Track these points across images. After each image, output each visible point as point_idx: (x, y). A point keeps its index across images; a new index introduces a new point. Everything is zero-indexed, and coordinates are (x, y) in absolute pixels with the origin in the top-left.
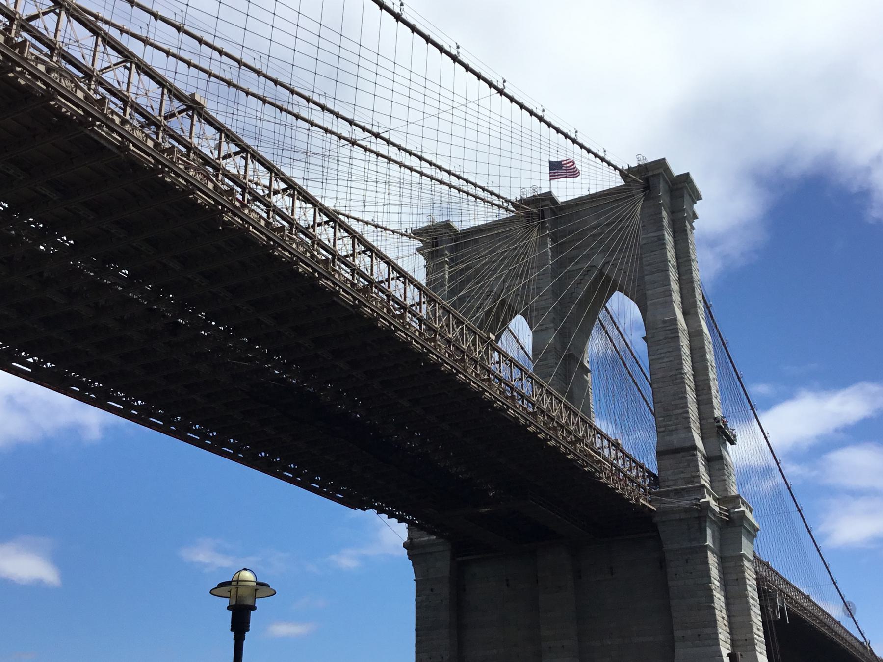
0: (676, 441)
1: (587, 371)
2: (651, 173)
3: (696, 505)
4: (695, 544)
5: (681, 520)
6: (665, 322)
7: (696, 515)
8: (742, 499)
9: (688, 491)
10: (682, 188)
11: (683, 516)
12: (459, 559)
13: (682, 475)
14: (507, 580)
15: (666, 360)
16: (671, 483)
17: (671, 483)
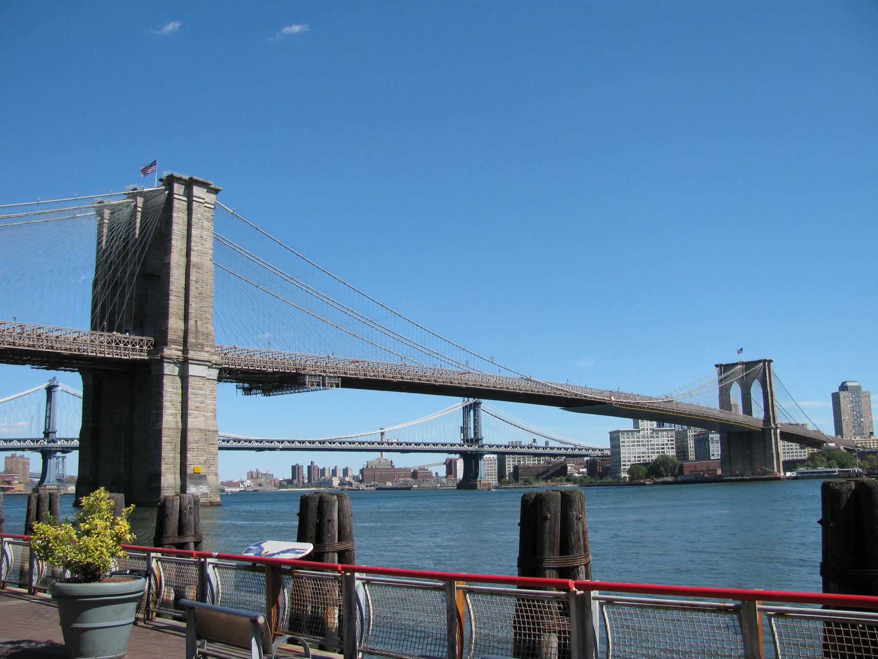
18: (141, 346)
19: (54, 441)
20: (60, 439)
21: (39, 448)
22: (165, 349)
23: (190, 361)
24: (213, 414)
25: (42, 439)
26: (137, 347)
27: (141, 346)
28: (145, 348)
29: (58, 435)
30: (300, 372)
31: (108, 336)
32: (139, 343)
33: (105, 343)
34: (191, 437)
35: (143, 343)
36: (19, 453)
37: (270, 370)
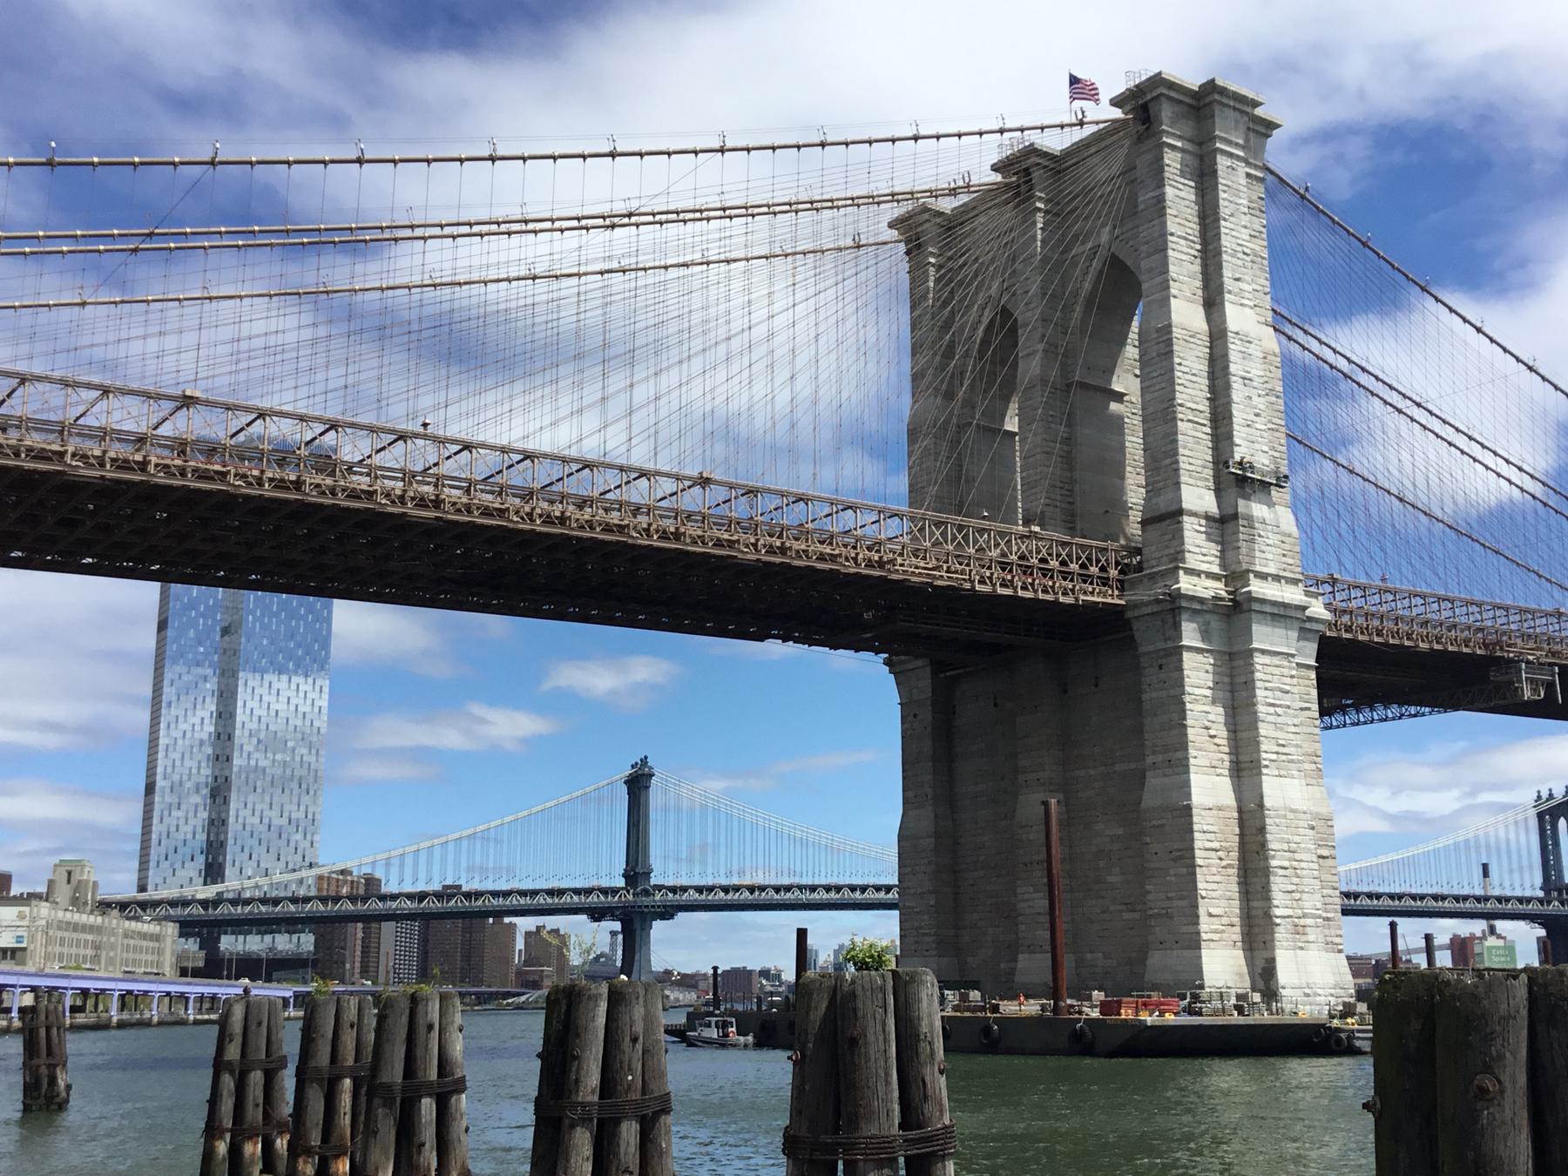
0: (1163, 505)
1: (1119, 397)
2: (1149, 97)
3: (1164, 594)
4: (1170, 644)
5: (1153, 614)
6: (1158, 330)
7: (1169, 607)
8: (1253, 571)
9: (1163, 574)
10: (1206, 105)
11: (1156, 608)
12: (942, 675)
13: (1166, 552)
14: (995, 698)
15: (1158, 387)
16: (1154, 562)
17: (1154, 562)
18: (1103, 569)
19: (646, 893)
20: (660, 888)
21: (617, 908)
22: (1181, 572)
23: (1256, 606)
24: (1314, 766)
25: (622, 889)
26: (1094, 570)
27: (1103, 569)
28: (1113, 573)
29: (653, 881)
30: (1498, 654)
31: (1022, 537)
32: (1098, 561)
33: (1014, 557)
34: (1276, 839)
35: (1107, 560)
36: (551, 922)
37: (1424, 646)
